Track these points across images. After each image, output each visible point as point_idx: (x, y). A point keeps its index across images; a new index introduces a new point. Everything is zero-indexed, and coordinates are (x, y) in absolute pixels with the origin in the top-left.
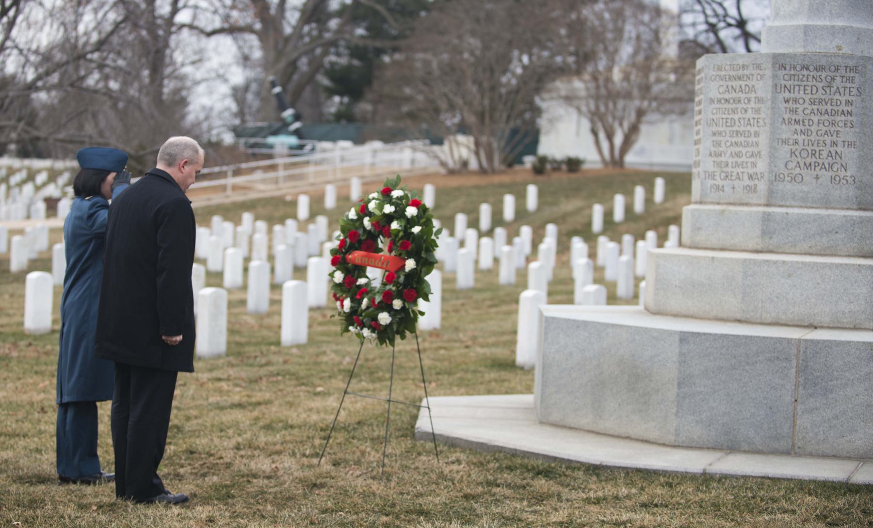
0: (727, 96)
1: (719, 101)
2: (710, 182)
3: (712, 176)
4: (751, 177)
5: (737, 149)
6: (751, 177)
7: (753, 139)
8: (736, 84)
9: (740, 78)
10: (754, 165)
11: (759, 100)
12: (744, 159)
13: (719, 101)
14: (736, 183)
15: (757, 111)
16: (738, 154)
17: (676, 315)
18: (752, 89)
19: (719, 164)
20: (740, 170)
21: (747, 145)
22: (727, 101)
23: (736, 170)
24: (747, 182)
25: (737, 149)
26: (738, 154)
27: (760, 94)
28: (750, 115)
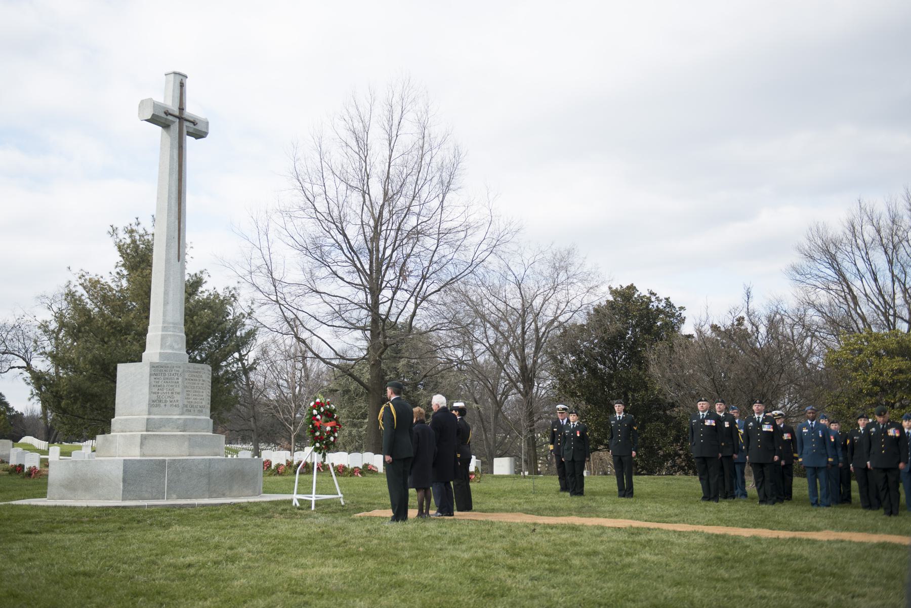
0: (192, 378)
1: (189, 380)
2: (185, 409)
3: (186, 406)
4: (200, 407)
5: (195, 397)
6: (200, 407)
7: (201, 394)
8: (195, 374)
9: (196, 372)
10: (202, 403)
11: (204, 381)
12: (198, 400)
13: (189, 380)
14: (195, 409)
15: (203, 384)
16: (196, 399)
17: (149, 456)
18: (201, 377)
19: (189, 402)
20: (196, 404)
21: (199, 396)
22: (192, 380)
23: (195, 404)
24: (199, 409)
25: (195, 397)
26: (196, 399)
27: (204, 379)
28: (200, 385)
